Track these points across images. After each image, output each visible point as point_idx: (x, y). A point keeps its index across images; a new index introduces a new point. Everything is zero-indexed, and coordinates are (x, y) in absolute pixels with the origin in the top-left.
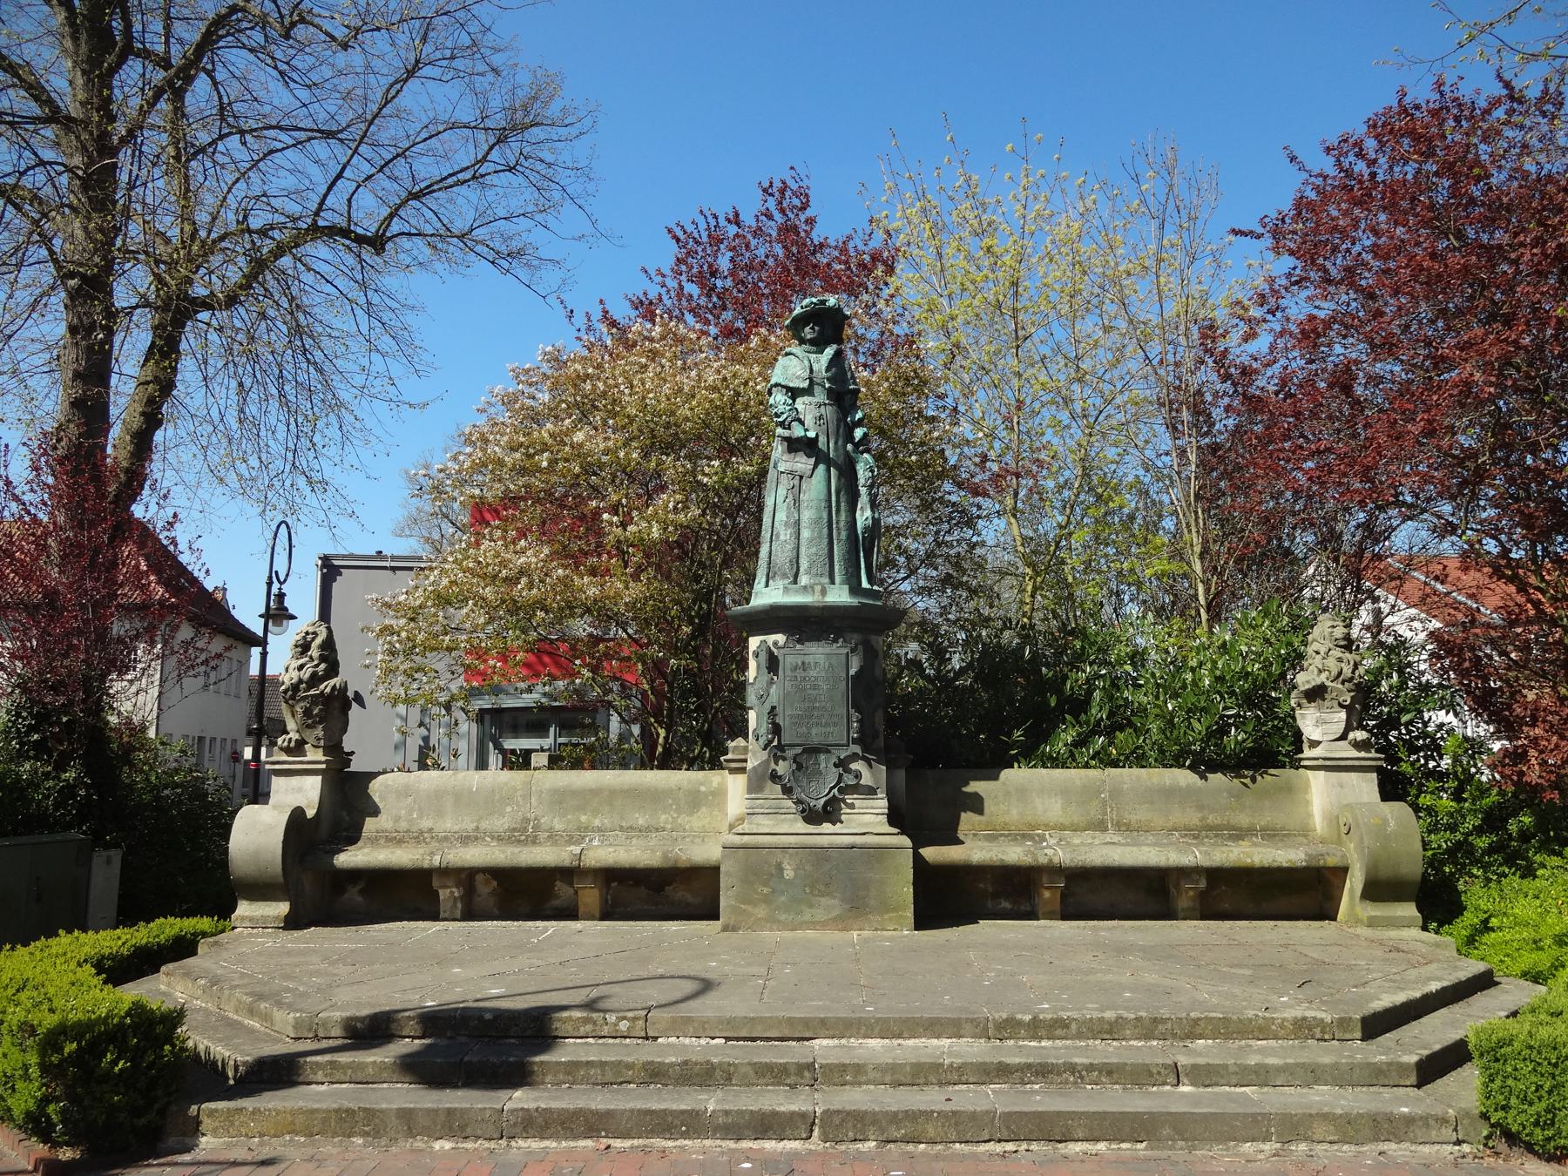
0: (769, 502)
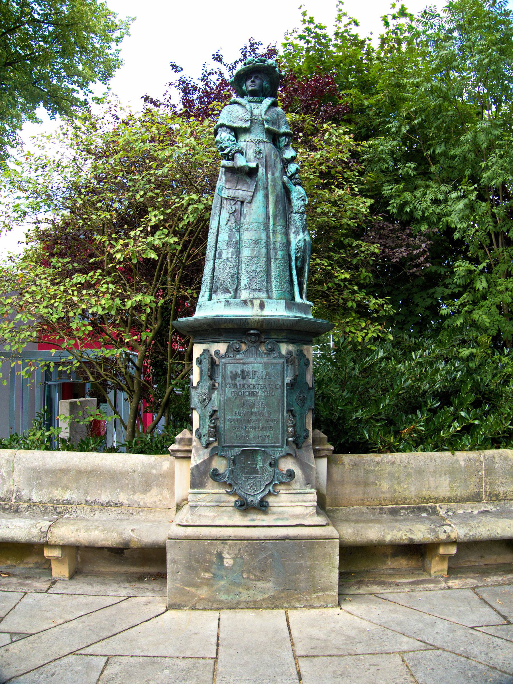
0: (213, 224)
